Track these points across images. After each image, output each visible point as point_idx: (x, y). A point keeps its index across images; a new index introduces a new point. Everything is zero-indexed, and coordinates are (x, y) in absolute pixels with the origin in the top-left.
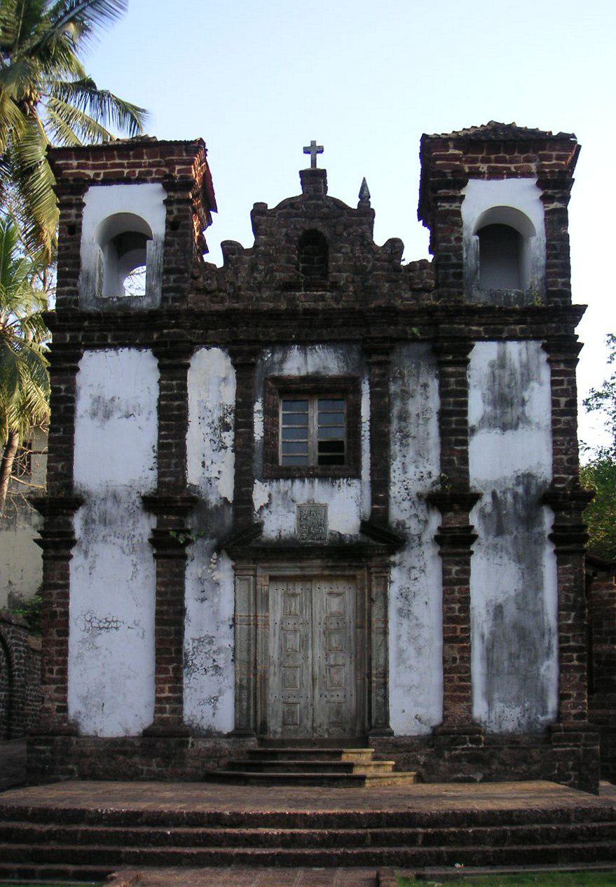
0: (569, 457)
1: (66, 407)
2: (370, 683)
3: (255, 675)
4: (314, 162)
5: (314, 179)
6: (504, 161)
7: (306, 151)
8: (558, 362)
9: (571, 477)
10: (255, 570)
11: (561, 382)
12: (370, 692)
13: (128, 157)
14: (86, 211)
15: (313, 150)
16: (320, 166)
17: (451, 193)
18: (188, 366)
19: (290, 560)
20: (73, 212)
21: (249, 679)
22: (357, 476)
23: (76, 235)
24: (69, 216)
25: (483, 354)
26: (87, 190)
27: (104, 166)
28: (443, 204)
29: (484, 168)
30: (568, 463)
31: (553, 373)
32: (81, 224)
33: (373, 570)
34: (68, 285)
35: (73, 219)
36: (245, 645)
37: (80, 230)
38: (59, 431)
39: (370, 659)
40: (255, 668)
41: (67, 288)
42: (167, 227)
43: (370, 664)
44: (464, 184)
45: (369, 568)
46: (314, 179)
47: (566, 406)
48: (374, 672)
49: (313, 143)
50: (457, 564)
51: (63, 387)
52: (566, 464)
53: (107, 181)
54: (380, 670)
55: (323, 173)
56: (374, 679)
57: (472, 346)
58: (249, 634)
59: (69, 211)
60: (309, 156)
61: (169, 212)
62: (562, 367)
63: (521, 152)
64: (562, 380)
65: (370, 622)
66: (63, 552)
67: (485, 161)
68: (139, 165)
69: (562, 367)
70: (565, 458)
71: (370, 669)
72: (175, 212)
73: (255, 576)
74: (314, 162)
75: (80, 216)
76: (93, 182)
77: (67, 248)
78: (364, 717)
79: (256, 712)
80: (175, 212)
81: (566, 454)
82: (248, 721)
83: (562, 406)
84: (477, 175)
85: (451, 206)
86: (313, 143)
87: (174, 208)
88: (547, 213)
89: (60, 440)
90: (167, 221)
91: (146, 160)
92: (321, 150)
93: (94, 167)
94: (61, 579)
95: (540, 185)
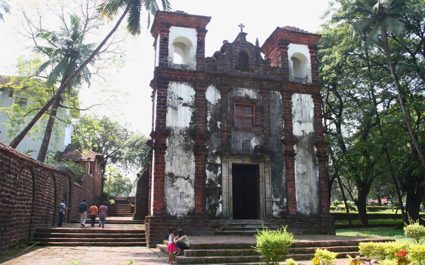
1: (163, 100)
2: (266, 201)
3: (229, 197)
4: (242, 30)
5: (242, 35)
7: (239, 26)
8: (317, 102)
10: (228, 161)
11: (318, 108)
12: (266, 204)
14: (170, 34)
15: (241, 26)
16: (244, 31)
17: (284, 46)
18: (206, 91)
19: (239, 158)
20: (166, 34)
21: (227, 199)
24: (164, 35)
25: (295, 97)
26: (170, 27)
31: (315, 105)
32: (168, 38)
33: (266, 163)
34: (164, 58)
35: (166, 36)
36: (225, 187)
37: (168, 40)
38: (161, 108)
39: (265, 193)
40: (229, 194)
41: (163, 59)
42: (197, 44)
43: (265, 194)
44: (288, 44)
45: (264, 162)
46: (242, 35)
48: (266, 197)
49: (242, 24)
50: (291, 162)
51: (162, 93)
54: (268, 196)
55: (245, 34)
56: (267, 199)
58: (227, 183)
59: (164, 33)
60: (240, 28)
61: (198, 39)
62: (318, 103)
65: (265, 180)
66: (162, 151)
69: (318, 103)
70: (320, 131)
71: (265, 196)
73: (228, 163)
74: (242, 30)
75: (168, 35)
76: (173, 25)
77: (164, 46)
78: (263, 212)
79: (229, 210)
80: (201, 39)
81: (320, 130)
82: (227, 213)
83: (318, 115)
86: (242, 24)
88: (312, 57)
89: (161, 111)
90: (198, 41)
92: (244, 26)
94: (162, 161)
95: (309, 48)
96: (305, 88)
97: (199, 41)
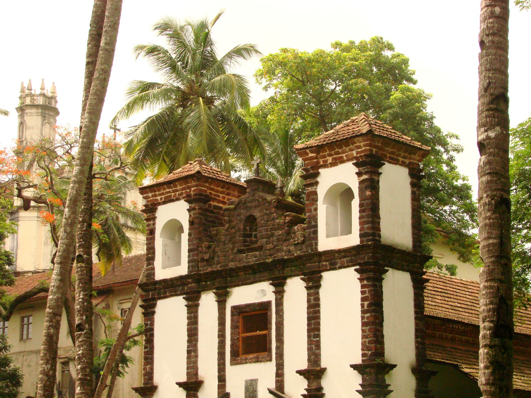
0: (369, 339)
6: (338, 153)
9: (370, 352)
13: (171, 188)
14: (157, 221)
20: (151, 222)
22: (270, 360)
23: (153, 235)
27: (163, 194)
28: (308, 189)
29: (330, 160)
30: (369, 343)
35: (152, 226)
47: (367, 307)
52: (367, 344)
53: (164, 203)
57: (321, 277)
63: (346, 146)
64: (366, 291)
67: (330, 155)
68: (177, 191)
72: (192, 215)
75: (154, 224)
76: (159, 204)
80: (192, 215)
81: (367, 338)
83: (366, 308)
84: (325, 166)
85: (312, 189)
87: (192, 213)
91: (179, 187)
93: (160, 195)
96: (344, 257)
97: (191, 220)
